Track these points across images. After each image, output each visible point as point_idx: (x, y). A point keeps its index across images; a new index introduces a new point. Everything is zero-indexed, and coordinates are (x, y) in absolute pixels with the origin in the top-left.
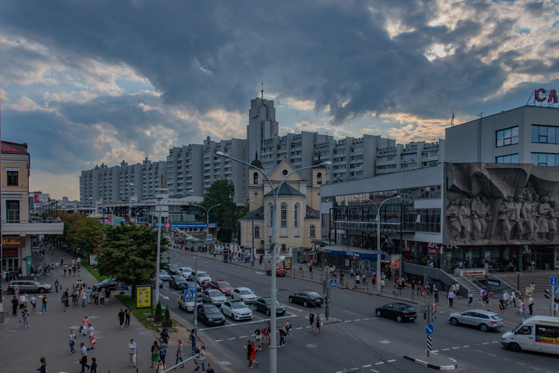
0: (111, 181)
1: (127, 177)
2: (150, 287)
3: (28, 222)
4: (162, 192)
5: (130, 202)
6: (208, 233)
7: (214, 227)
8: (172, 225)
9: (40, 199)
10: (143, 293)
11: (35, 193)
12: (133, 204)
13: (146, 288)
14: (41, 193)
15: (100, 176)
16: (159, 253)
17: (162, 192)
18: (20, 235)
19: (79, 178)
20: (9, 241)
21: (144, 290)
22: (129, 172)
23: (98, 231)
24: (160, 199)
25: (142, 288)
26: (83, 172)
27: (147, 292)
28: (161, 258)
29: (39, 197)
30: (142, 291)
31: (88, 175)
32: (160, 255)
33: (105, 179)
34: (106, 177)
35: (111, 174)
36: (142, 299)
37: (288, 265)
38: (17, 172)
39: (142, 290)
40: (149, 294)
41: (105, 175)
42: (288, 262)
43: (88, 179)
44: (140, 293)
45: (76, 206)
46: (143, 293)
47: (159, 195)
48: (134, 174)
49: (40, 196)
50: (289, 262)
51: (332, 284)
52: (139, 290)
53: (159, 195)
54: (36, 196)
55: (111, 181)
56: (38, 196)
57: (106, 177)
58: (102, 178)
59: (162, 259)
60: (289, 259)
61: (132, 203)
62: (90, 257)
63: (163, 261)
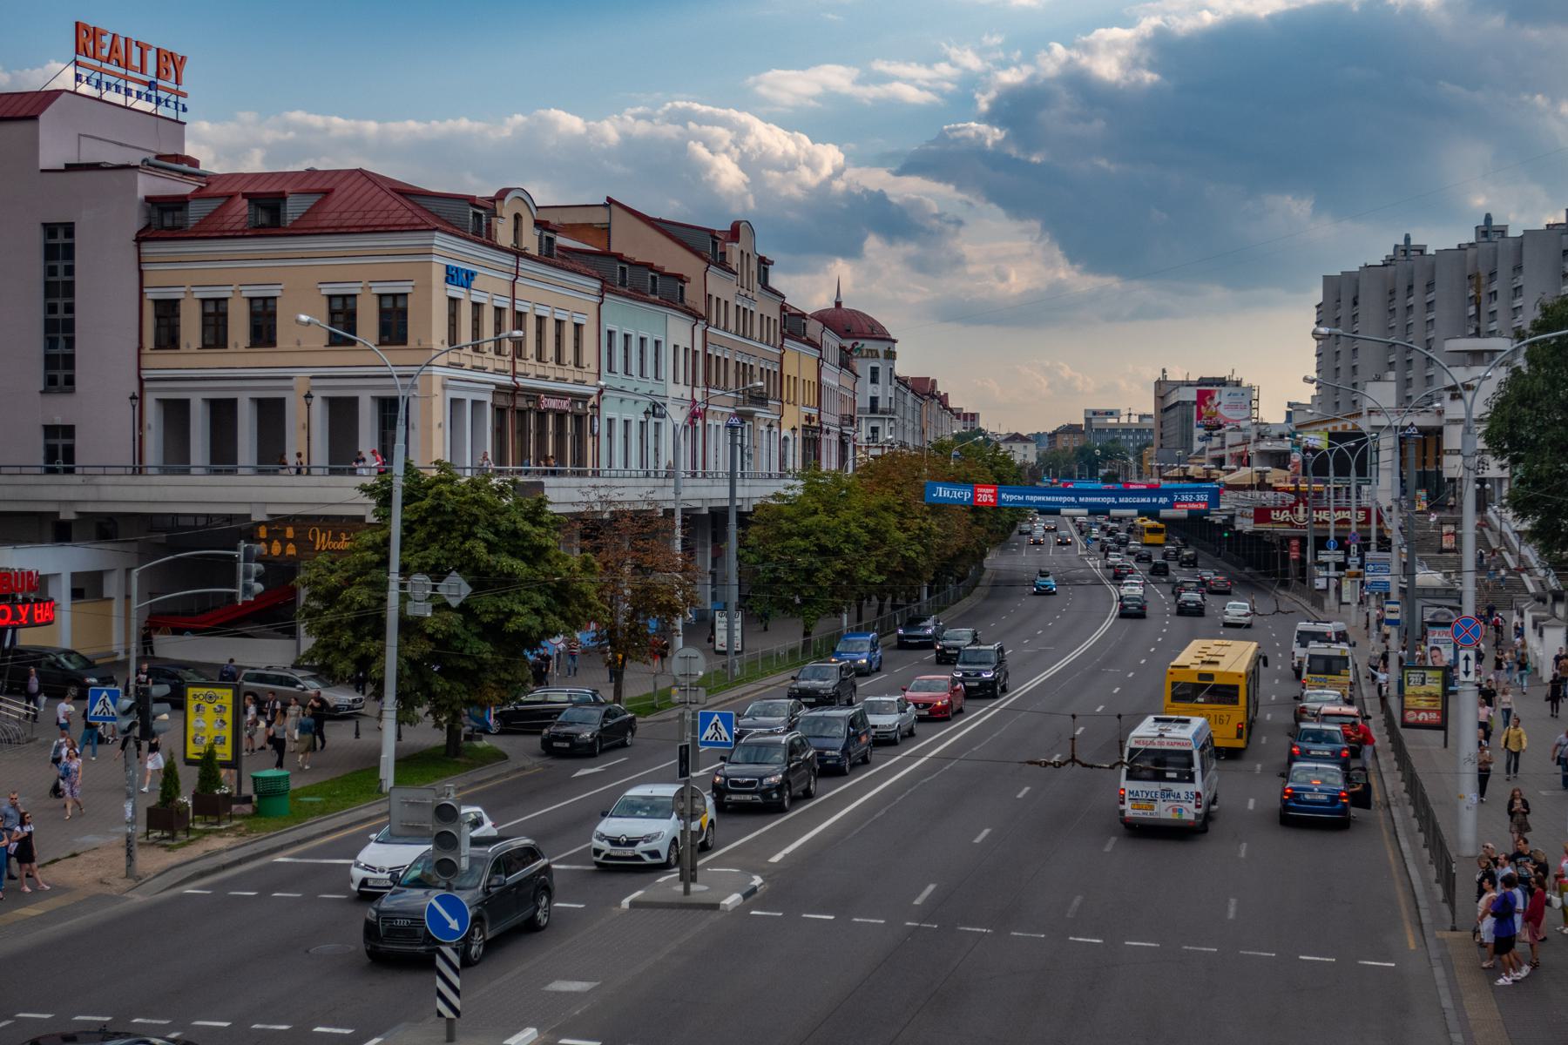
0: (1431, 316)
1: (1495, 292)
2: (230, 692)
3: (327, 470)
4: (1477, 356)
5: (1365, 413)
6: (1373, 547)
7: (1202, 506)
8: (1003, 496)
9: (1221, 409)
10: (209, 708)
11: (1202, 382)
12: (1377, 420)
13: (218, 691)
14: (1222, 382)
15: (1392, 292)
16: (394, 578)
17: (1477, 356)
18: (249, 516)
19: (1315, 310)
20: (336, 537)
21: (210, 699)
22: (1504, 269)
23: (807, 522)
24: (1455, 392)
25: (205, 691)
26: (1328, 281)
27: (220, 706)
28: (404, 598)
29: (1217, 400)
30: (204, 704)
31: (1346, 299)
32: (403, 586)
33: (1410, 308)
34: (1411, 301)
35: (1430, 286)
36: (202, 729)
37: (1423, 704)
38: (405, 295)
39: (205, 697)
40: (228, 716)
41: (1410, 287)
42: (1422, 690)
43: (1345, 311)
44: (198, 707)
45: (1254, 437)
46: (209, 708)
47: (1460, 375)
48: (1521, 281)
49: (1222, 396)
50: (1436, 688)
51: (709, 732)
52: (195, 697)
53: (1460, 375)
54: (1203, 397)
55: (1431, 316)
56: (1212, 398)
57: (1411, 301)
58: (1398, 305)
59: (410, 599)
60: (1429, 674)
61: (1370, 412)
62: (717, 618)
63: (413, 610)
